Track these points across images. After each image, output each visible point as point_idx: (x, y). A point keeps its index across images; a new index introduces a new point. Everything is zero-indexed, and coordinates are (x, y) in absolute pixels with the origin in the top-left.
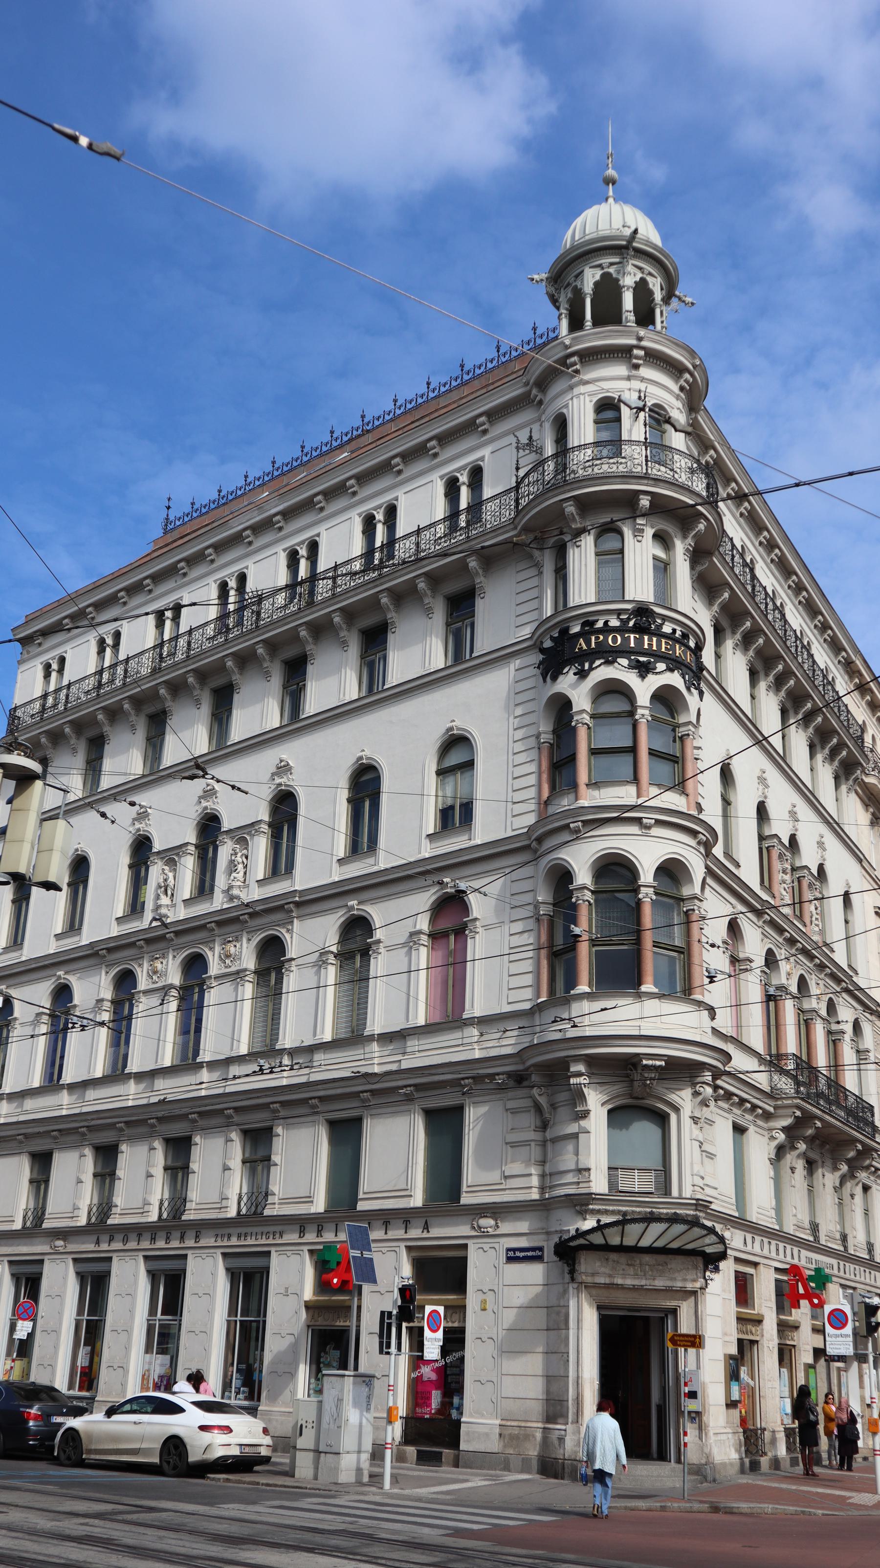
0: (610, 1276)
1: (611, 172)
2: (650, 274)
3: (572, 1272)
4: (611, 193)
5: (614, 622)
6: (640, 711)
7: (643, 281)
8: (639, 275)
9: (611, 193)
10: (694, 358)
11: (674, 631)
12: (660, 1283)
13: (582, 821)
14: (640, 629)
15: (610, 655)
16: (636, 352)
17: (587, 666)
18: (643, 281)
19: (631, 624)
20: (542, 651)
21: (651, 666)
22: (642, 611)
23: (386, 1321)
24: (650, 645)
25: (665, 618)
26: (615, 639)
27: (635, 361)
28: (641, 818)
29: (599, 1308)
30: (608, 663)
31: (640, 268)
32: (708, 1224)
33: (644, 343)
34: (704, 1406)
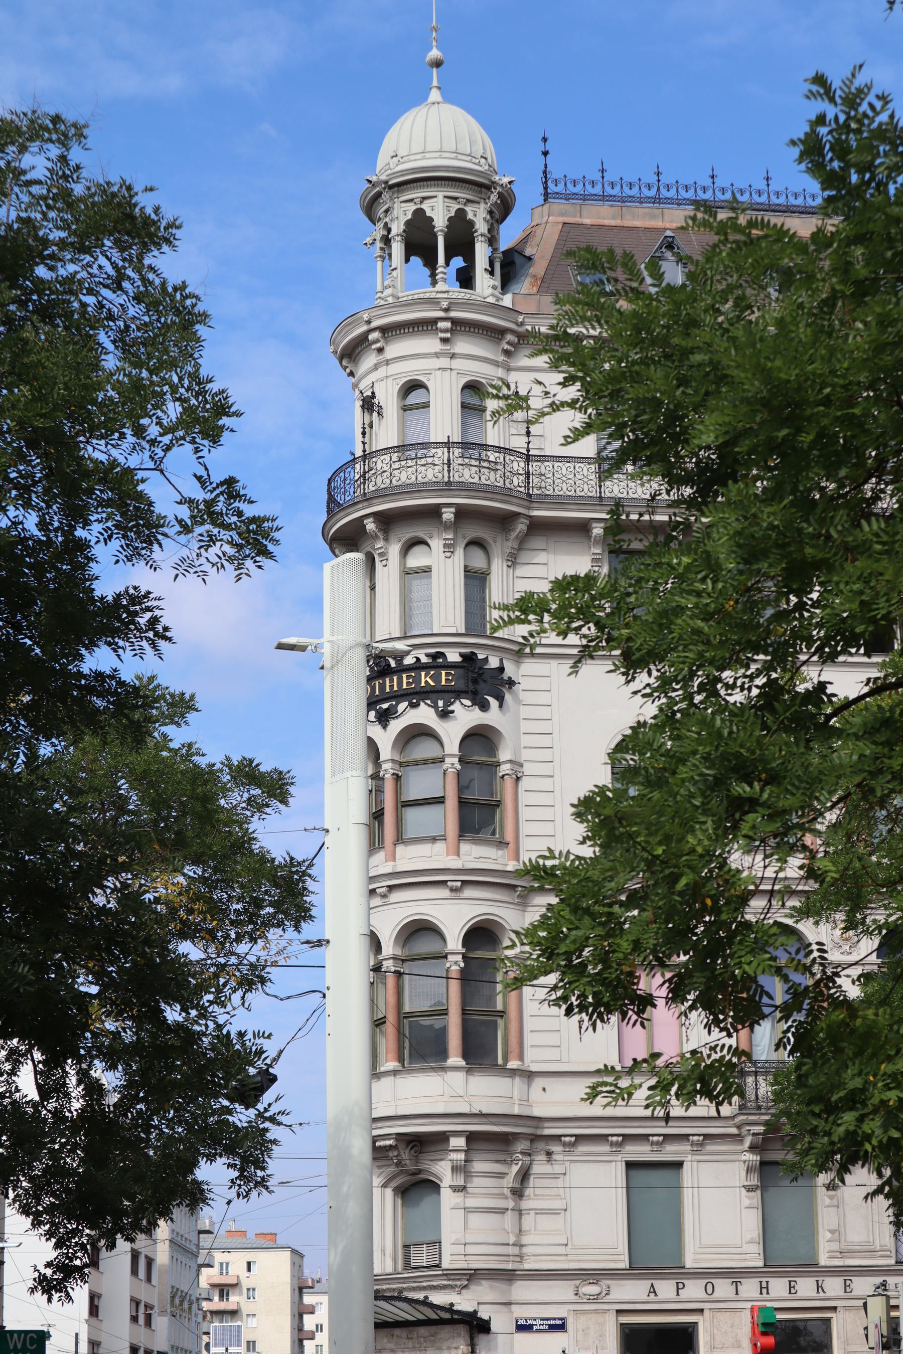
2: (424, 198)
4: (435, 83)
7: (419, 213)
8: (412, 207)
9: (435, 83)
10: (439, 303)
11: (418, 659)
18: (419, 213)
24: (391, 686)
27: (373, 347)
31: (411, 200)
32: (419, 1296)
33: (375, 324)
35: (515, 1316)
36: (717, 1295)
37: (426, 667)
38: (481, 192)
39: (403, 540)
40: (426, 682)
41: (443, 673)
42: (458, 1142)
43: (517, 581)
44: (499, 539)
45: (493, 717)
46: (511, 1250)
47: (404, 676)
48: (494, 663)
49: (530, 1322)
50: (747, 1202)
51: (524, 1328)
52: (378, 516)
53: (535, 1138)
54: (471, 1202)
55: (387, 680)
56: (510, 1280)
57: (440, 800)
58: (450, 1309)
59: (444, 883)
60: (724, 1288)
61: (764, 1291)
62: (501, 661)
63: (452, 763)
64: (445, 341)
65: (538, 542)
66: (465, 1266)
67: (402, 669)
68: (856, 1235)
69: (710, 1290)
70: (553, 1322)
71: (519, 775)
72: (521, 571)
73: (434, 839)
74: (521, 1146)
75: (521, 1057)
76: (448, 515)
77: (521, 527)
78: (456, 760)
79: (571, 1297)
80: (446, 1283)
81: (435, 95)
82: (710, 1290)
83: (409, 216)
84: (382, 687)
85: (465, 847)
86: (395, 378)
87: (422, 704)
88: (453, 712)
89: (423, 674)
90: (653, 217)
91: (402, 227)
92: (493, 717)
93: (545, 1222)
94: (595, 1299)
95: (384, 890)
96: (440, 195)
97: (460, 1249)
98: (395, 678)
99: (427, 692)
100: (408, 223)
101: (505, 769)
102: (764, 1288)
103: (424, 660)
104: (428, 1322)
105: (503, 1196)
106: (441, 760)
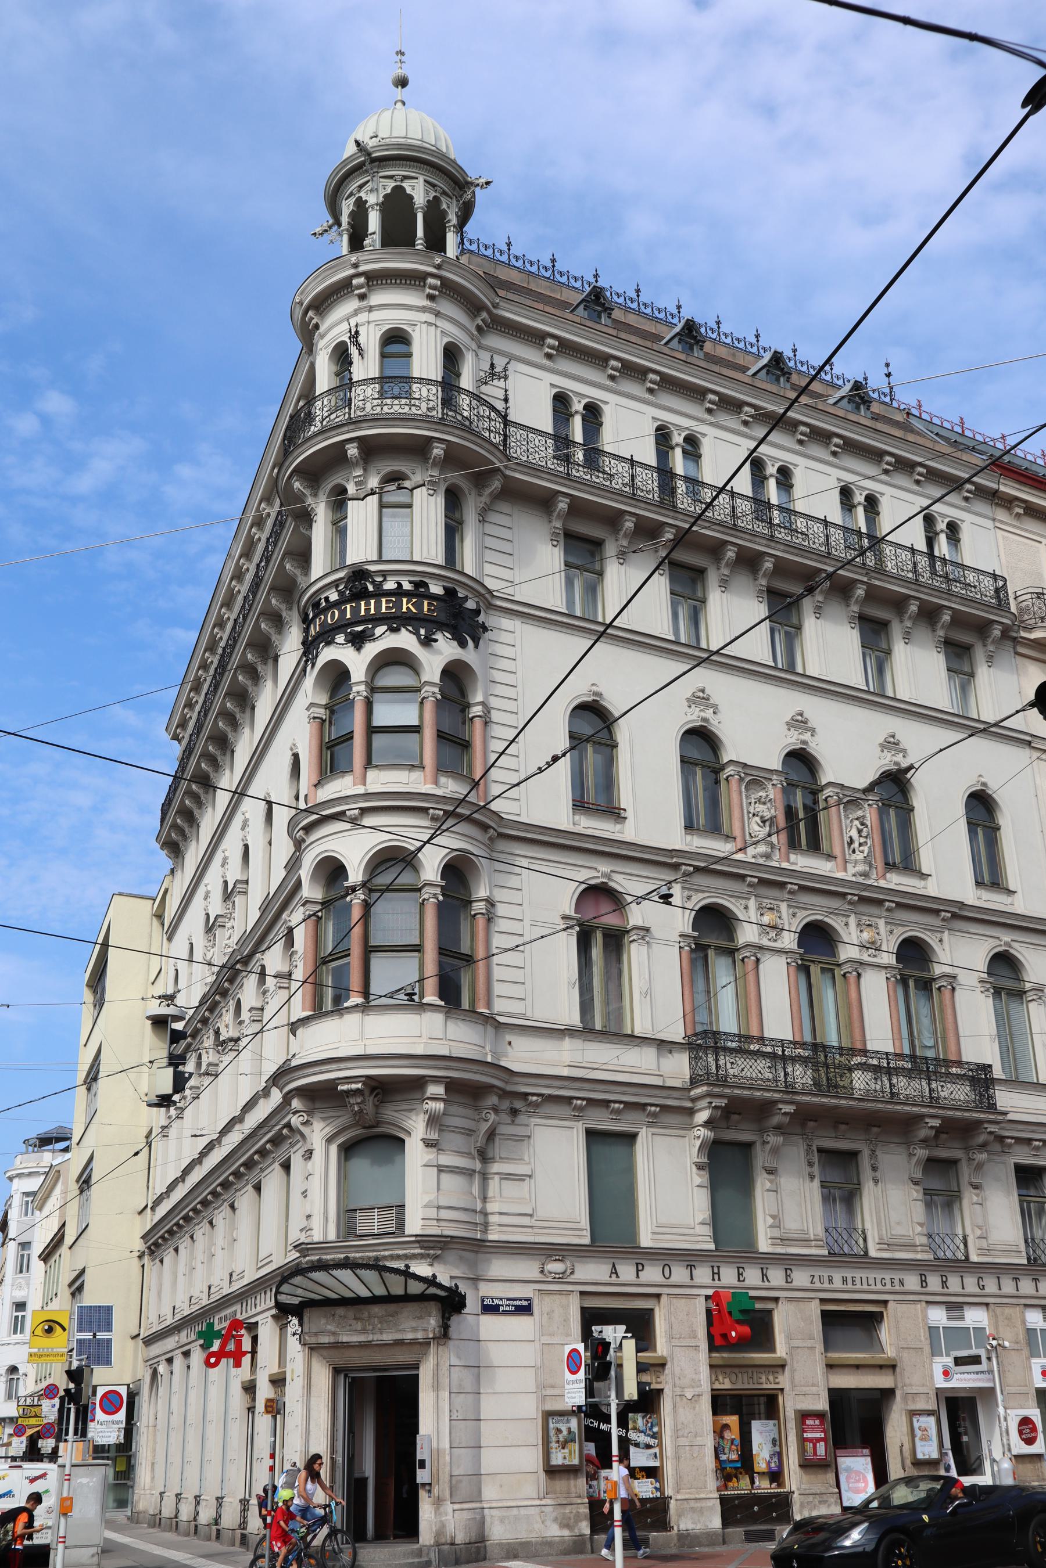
0: (334, 1334)
2: (405, 178)
6: (355, 689)
7: (399, 190)
8: (391, 184)
11: (400, 585)
12: (388, 1336)
13: (302, 828)
14: (362, 595)
16: (355, 282)
18: (399, 190)
21: (368, 633)
22: (359, 574)
23: (66, 1406)
24: (367, 610)
25: (385, 574)
27: (357, 292)
28: (343, 813)
29: (337, 1371)
30: (329, 643)
32: (400, 1265)
34: (436, 1475)
35: (480, 1295)
36: (675, 1278)
37: (408, 594)
38: (454, 189)
39: (383, 473)
40: (408, 608)
41: (426, 603)
42: (436, 1090)
43: (487, 538)
44: (473, 493)
45: (469, 655)
46: (478, 1219)
47: (384, 600)
48: (471, 605)
49: (496, 1302)
50: (698, 1180)
51: (490, 1309)
52: (362, 442)
53: (505, 1094)
54: (445, 1160)
55: (363, 603)
56: (477, 1252)
57: (416, 729)
58: (432, 1281)
59: (425, 810)
60: (679, 1274)
61: (716, 1277)
62: (478, 603)
63: (431, 692)
64: (431, 298)
65: (504, 507)
66: (439, 1232)
67: (380, 593)
68: (792, 1224)
69: (667, 1274)
70: (519, 1303)
71: (488, 720)
72: (489, 529)
73: (413, 767)
74: (493, 1100)
75: (489, 1004)
76: (438, 451)
77: (496, 484)
78: (436, 690)
79: (535, 1275)
80: (417, 1251)
82: (667, 1274)
83: (389, 191)
84: (356, 610)
85: (443, 780)
86: (378, 323)
87: (403, 630)
88: (436, 641)
89: (405, 600)
90: (553, 291)
91: (381, 199)
92: (469, 655)
93: (511, 1188)
94: (560, 1278)
95: (356, 812)
96: (421, 179)
97: (432, 1213)
98: (372, 602)
99: (410, 618)
100: (386, 196)
101: (476, 710)
102: (716, 1274)
103: (407, 586)
104: (389, 1299)
105: (469, 1155)
106: (417, 690)
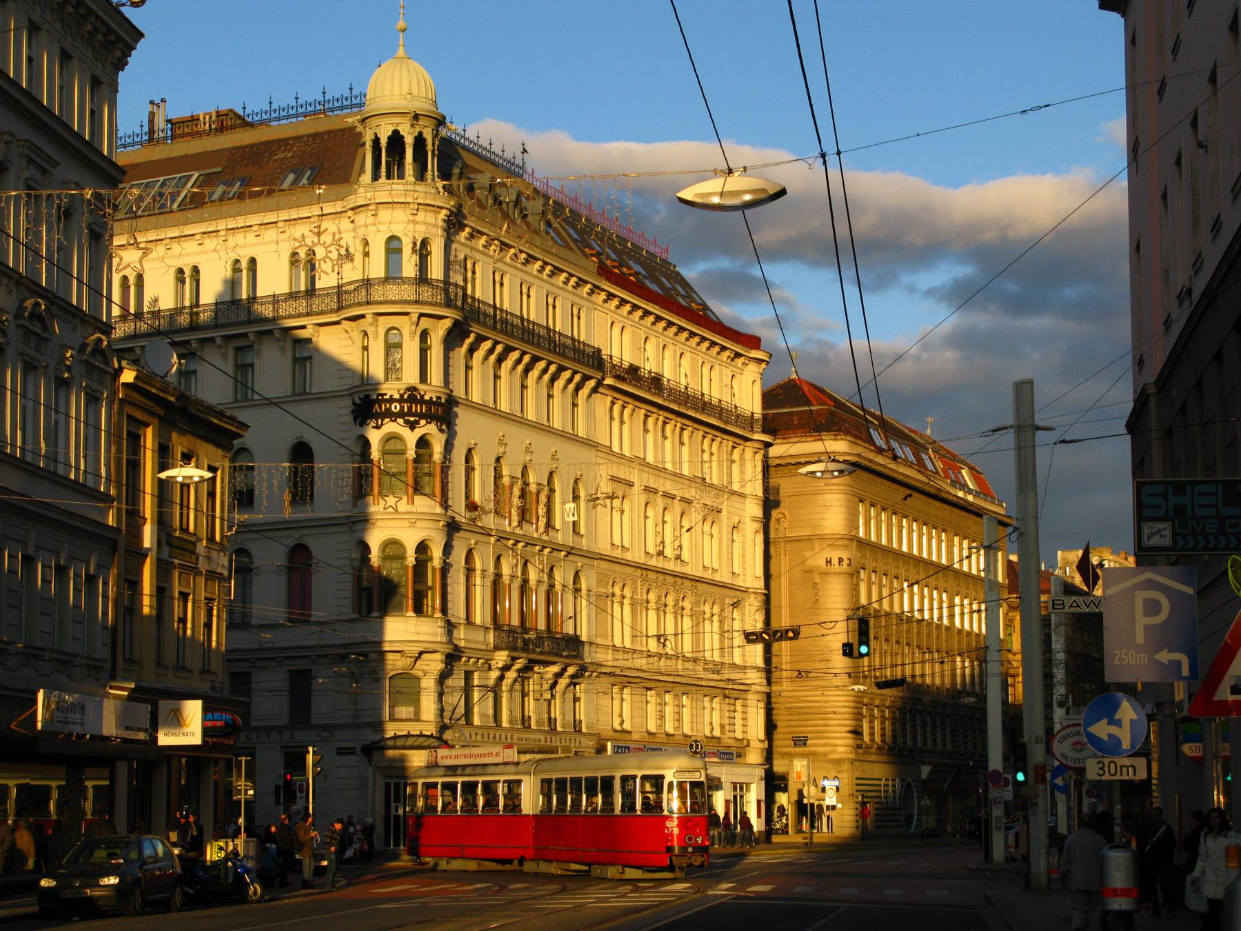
1: (401, 24)
3: (370, 761)
4: (401, 43)
5: (397, 396)
9: (401, 43)
15: (393, 416)
17: (380, 421)
19: (406, 396)
20: (354, 403)
26: (396, 407)
81: (401, 52)
84: (410, 408)
103: (434, 399)
